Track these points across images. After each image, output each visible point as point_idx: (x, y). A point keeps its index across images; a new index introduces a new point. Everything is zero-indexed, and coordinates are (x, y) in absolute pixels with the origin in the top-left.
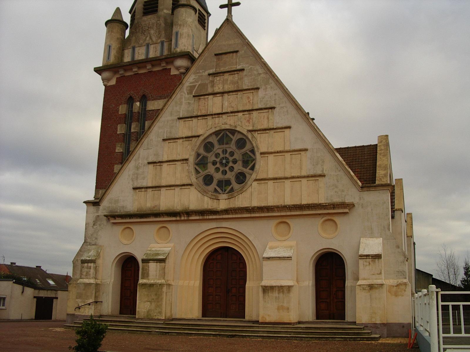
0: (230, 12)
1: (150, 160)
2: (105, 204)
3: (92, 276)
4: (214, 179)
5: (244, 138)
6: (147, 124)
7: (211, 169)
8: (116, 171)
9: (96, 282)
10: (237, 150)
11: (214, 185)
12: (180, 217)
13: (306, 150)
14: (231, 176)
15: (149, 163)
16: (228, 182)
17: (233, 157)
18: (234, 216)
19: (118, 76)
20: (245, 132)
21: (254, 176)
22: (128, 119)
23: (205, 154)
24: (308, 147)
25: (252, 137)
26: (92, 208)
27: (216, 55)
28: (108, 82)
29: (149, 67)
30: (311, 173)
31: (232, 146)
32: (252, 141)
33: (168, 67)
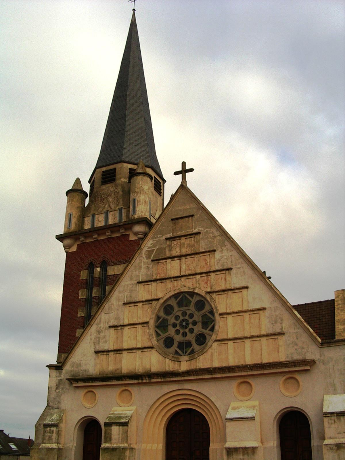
0: (184, 178)
1: (111, 324)
2: (68, 367)
3: (54, 440)
4: (175, 341)
5: (203, 299)
6: (108, 288)
7: (171, 332)
8: (78, 335)
9: (58, 447)
10: (196, 312)
11: (175, 347)
12: (142, 380)
13: (264, 309)
14: (191, 337)
15: (110, 327)
16: (188, 344)
17: (193, 319)
18: (195, 377)
19: (79, 243)
20: (203, 294)
21: (214, 337)
22: (89, 284)
23: (166, 317)
25: (210, 299)
26: (55, 373)
27: (172, 220)
28: (69, 249)
29: (108, 233)
30: (271, 331)
31: (192, 309)
32: (210, 302)
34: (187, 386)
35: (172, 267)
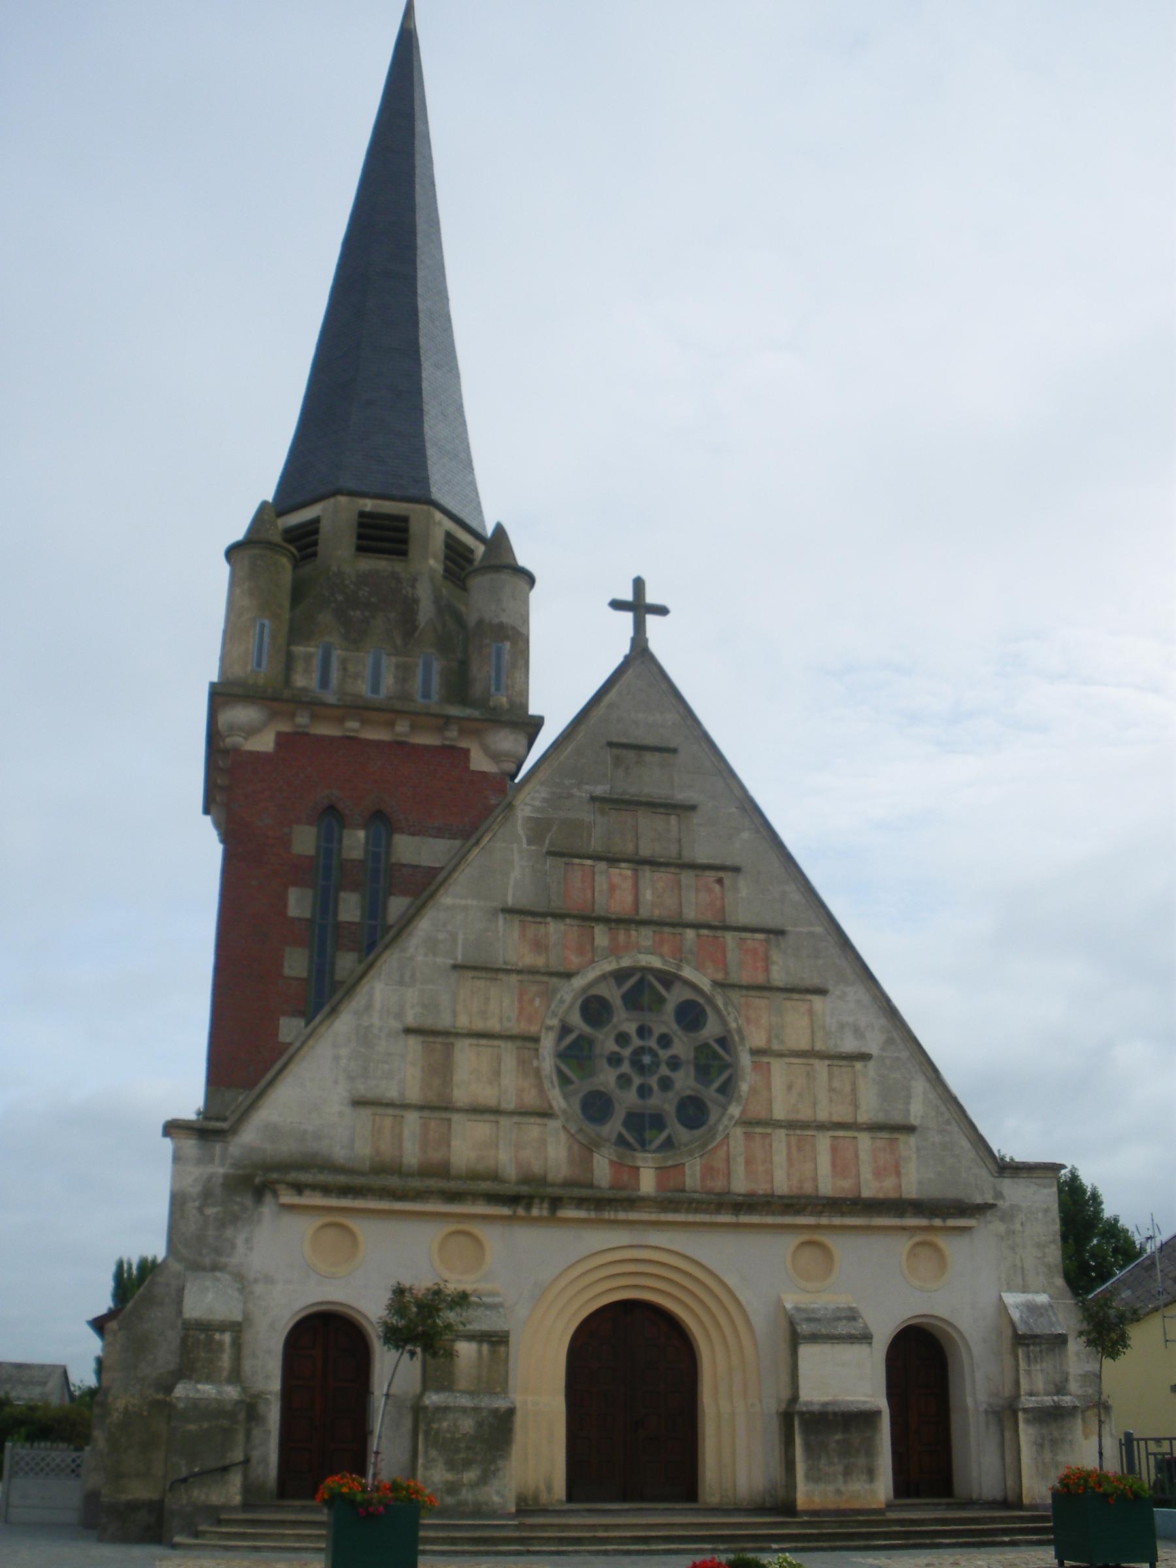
0: (639, 627)
1: (410, 1019)
2: (249, 1137)
3: (225, 1374)
4: (617, 1106)
5: (701, 1001)
6: (397, 905)
7: (607, 1078)
10: (679, 1033)
11: (614, 1126)
12: (528, 1207)
13: (864, 1057)
14: (665, 1103)
15: (408, 1031)
16: (658, 1122)
17: (670, 1052)
19: (285, 727)
20: (705, 984)
21: (735, 1110)
22: (327, 876)
23: (587, 1029)
24: (873, 1048)
25: (726, 1004)
26: (191, 1145)
27: (611, 744)
28: (246, 739)
29: (402, 727)
30: (881, 1118)
31: (665, 1022)
32: (725, 1013)
33: (463, 744)
35: (612, 888)
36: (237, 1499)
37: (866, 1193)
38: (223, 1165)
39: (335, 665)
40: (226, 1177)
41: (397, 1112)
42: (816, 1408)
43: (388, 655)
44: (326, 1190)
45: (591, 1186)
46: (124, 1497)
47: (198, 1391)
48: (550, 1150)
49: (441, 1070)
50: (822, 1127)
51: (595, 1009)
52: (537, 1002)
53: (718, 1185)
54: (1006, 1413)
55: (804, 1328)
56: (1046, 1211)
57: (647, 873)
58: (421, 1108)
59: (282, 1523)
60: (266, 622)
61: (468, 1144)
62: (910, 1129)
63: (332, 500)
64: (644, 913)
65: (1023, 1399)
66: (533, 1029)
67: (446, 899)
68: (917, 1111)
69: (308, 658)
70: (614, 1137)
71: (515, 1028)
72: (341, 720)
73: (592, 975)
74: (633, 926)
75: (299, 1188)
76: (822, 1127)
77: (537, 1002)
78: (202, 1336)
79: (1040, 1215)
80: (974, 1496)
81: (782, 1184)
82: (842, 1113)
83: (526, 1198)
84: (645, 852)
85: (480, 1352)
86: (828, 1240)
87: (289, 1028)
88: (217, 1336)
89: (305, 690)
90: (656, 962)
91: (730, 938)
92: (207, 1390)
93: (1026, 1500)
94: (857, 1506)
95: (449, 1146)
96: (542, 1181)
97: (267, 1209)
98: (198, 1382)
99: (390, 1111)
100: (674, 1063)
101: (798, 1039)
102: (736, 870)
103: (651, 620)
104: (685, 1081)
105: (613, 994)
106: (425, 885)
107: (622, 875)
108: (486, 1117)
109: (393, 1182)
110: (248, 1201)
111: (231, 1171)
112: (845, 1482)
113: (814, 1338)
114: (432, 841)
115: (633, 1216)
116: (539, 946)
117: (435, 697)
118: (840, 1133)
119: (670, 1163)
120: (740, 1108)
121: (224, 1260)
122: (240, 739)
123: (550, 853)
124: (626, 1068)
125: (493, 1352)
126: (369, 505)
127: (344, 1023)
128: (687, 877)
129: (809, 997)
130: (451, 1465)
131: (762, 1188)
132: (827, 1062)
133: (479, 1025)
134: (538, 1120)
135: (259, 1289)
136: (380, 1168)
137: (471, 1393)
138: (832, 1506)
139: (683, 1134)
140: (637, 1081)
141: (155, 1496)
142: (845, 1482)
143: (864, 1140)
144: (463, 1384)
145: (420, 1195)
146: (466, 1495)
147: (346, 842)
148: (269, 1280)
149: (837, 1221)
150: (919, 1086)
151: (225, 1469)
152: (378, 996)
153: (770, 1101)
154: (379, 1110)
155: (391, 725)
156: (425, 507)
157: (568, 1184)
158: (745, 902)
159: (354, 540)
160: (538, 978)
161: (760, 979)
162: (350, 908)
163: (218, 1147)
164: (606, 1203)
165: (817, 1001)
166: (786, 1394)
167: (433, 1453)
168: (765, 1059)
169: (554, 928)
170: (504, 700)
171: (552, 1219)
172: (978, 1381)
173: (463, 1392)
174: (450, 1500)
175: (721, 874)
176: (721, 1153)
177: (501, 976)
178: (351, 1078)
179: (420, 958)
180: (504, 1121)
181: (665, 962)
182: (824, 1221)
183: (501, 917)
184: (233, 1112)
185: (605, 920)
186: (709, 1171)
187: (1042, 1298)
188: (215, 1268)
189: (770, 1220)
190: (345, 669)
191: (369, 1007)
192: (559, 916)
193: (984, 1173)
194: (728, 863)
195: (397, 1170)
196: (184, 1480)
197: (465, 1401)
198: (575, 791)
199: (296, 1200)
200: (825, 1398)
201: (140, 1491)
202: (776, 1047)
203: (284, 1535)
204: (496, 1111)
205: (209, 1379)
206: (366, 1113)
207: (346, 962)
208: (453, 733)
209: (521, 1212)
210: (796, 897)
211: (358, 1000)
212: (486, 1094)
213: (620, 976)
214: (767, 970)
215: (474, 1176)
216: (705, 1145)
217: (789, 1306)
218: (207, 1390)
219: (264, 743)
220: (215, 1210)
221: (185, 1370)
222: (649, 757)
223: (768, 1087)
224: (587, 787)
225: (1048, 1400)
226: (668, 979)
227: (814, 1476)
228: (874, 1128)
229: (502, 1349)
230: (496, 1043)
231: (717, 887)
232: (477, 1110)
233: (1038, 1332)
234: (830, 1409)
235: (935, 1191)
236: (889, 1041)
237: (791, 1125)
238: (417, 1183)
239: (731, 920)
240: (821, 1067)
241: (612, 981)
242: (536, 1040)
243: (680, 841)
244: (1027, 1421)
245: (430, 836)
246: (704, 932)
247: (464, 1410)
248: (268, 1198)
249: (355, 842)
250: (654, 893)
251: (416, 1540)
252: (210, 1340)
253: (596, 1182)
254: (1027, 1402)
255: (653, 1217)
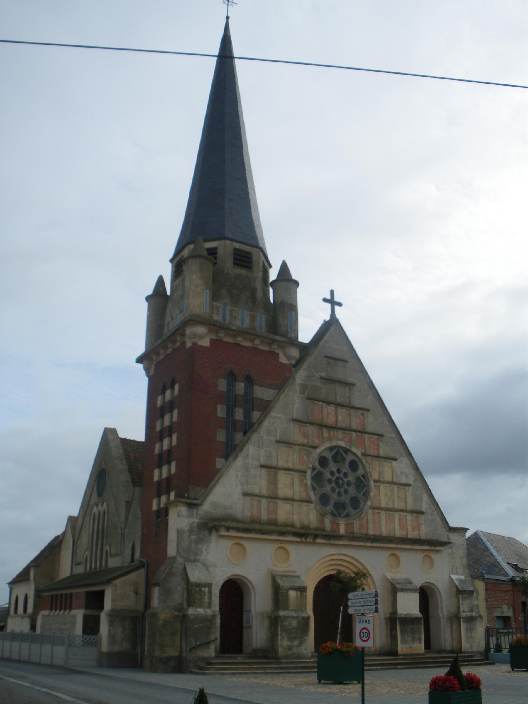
1: (262, 462)
3: (206, 604)
5: (357, 460)
6: (256, 415)
7: (327, 488)
8: (218, 466)
9: (205, 612)
10: (351, 472)
11: (330, 507)
12: (306, 538)
13: (409, 485)
14: (346, 499)
15: (262, 466)
18: (346, 543)
19: (214, 337)
20: (359, 455)
21: (369, 503)
23: (321, 469)
24: (411, 482)
25: (366, 462)
27: (326, 357)
30: (413, 508)
31: (346, 468)
34: (345, 551)
35: (328, 414)
36: (213, 655)
37: (410, 536)
38: (197, 518)
39: (228, 313)
40: (198, 523)
41: (259, 499)
42: (403, 616)
43: (247, 310)
44: (238, 530)
45: (324, 530)
46: (165, 655)
47: (197, 611)
48: (309, 515)
49: (273, 482)
50: (396, 511)
51: (323, 461)
52: (305, 457)
53: (364, 531)
54: (455, 618)
55: (397, 586)
56: (463, 545)
57: (340, 410)
58: (267, 497)
59: (234, 663)
60: (208, 291)
61: (284, 513)
62: (422, 513)
63: (223, 241)
64: (339, 425)
65: (461, 613)
66: (304, 468)
67: (273, 414)
68: (425, 506)
69: (218, 308)
70: (330, 511)
71: (298, 467)
72: (235, 336)
73: (323, 448)
74: (336, 430)
75: (228, 529)
76: (396, 511)
77: (305, 457)
78: (198, 589)
79: (461, 547)
80: (443, 649)
81: (384, 532)
82: (401, 506)
83: (305, 534)
84: (339, 401)
85: (297, 594)
86: (398, 553)
87: (219, 462)
88: (203, 589)
89: (217, 321)
90: (343, 444)
91: (366, 436)
92: (200, 611)
93: (463, 650)
94: (416, 652)
95: (277, 513)
96: (308, 528)
97: (214, 536)
98: (196, 608)
99: (256, 498)
100: (349, 484)
101: (388, 477)
102: (368, 410)
103: (336, 307)
104: (352, 491)
105: (329, 456)
106: (266, 407)
107: (331, 409)
108: (290, 502)
109: (258, 527)
110: (206, 533)
111: (200, 521)
112: (413, 643)
113: (402, 590)
114: (267, 389)
115: (340, 542)
116: (305, 435)
117: (264, 330)
118: (401, 513)
119: (349, 522)
120: (371, 502)
121: (198, 557)
122: (197, 340)
123: (308, 398)
124: (333, 485)
125: (301, 595)
126: (238, 246)
127: (239, 462)
128: (352, 412)
129: (391, 461)
130: (290, 639)
131: (378, 533)
132: (397, 486)
133: (286, 465)
134: (307, 504)
135: (211, 569)
136: (254, 521)
137: (295, 611)
138: (409, 652)
139: (353, 511)
140: (337, 490)
141: (177, 654)
142: (413, 643)
143: (409, 516)
144: (292, 607)
145: (271, 533)
146: (295, 650)
147: (237, 387)
148: (215, 566)
149: (403, 546)
150: (425, 497)
151: (209, 643)
152: (251, 451)
153: (380, 500)
154: (253, 498)
155: (253, 340)
156: (258, 250)
157: (316, 529)
158: (372, 423)
159: (233, 260)
160: (305, 448)
161: (376, 453)
162: (239, 415)
163: (195, 511)
164: (332, 537)
165: (394, 463)
166: (390, 610)
167: (284, 634)
168: (378, 484)
169: (310, 429)
170: (293, 335)
171: (314, 543)
172: (444, 605)
173: (292, 610)
174: (289, 653)
175: (363, 412)
176: (365, 519)
177: (293, 446)
178: (242, 484)
179: (265, 437)
180: (296, 504)
181: (346, 445)
182: (399, 546)
183: (292, 422)
184: (200, 496)
185: (327, 426)
186: (361, 525)
187: (462, 577)
188: (195, 561)
189: (382, 545)
190: (231, 315)
191: (247, 456)
192: (311, 424)
193: (444, 530)
194: (365, 407)
195: (260, 522)
196: (194, 648)
197: (293, 614)
198: (315, 374)
199: (226, 533)
200: (406, 613)
201: (172, 652)
202: (381, 479)
203: (239, 668)
204: (293, 500)
205: (200, 607)
206: (248, 499)
207: (239, 437)
208: (275, 346)
209: (304, 540)
210: (387, 422)
211: (243, 454)
212: (289, 493)
213: (331, 449)
214: (378, 450)
215: (285, 525)
216: (360, 516)
217: (389, 578)
218: (200, 611)
219: (206, 343)
220: (194, 537)
221: (190, 603)
222: (339, 363)
223: (379, 495)
224: (320, 373)
225: (469, 614)
226: (347, 451)
227: (404, 642)
228: (412, 512)
229: (304, 594)
230: (292, 473)
231: (362, 417)
232: (286, 499)
233: (465, 589)
234: (407, 616)
235: (430, 537)
236: (416, 480)
237: (387, 510)
238: (248, 526)
239: (367, 430)
240: (395, 488)
241: (328, 451)
242: (305, 472)
243: (350, 397)
244: (463, 622)
245: (267, 387)
246: (358, 434)
247: (293, 617)
248: (214, 532)
249: (240, 387)
250: (342, 417)
251: (363, 665)
252: (200, 590)
253: (326, 529)
254: (463, 615)
255: (346, 543)
